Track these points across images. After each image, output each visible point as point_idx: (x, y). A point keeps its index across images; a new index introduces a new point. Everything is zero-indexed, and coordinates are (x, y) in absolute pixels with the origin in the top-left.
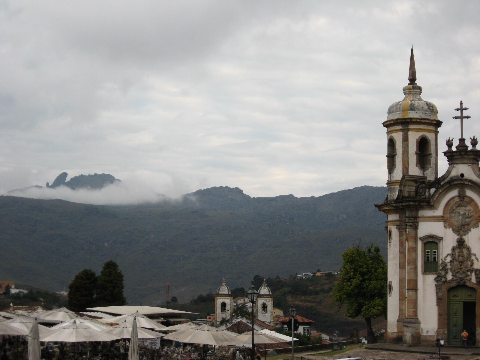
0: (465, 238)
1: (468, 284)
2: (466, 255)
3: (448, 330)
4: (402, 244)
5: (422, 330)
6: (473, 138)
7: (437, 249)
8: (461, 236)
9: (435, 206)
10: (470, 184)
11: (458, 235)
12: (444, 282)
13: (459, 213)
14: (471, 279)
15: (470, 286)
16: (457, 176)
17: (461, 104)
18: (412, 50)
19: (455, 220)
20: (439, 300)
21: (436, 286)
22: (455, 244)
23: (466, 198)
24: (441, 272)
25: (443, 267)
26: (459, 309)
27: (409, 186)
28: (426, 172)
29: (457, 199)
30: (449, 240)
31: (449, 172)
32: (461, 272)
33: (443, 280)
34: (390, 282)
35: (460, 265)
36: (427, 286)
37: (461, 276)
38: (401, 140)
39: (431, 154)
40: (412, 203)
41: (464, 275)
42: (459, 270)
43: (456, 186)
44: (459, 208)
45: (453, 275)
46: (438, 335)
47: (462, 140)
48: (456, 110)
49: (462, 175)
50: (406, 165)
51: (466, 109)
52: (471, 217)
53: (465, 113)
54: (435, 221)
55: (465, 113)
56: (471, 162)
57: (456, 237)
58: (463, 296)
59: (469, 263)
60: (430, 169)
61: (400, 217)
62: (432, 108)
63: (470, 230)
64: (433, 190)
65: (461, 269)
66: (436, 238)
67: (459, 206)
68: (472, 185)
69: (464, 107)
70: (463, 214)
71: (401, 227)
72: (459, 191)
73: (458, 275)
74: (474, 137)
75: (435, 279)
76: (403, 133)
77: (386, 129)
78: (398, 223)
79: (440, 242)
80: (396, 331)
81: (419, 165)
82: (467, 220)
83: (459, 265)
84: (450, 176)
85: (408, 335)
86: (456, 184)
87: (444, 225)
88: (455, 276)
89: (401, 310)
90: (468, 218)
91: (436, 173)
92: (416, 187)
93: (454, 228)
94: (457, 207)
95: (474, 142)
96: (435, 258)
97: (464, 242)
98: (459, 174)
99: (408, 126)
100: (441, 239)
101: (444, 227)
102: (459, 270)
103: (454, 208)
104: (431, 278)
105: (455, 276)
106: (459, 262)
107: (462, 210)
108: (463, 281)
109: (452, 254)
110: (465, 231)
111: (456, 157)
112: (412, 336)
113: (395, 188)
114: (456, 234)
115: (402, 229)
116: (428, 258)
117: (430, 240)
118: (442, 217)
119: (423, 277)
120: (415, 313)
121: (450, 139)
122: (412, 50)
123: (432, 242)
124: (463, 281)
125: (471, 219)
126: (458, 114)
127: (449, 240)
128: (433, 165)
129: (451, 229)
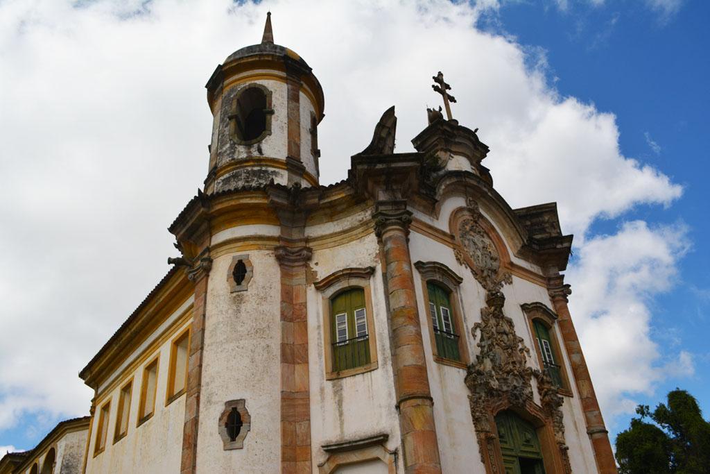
10: (489, 194)
11: (484, 287)
14: (532, 393)
15: (533, 414)
17: (440, 74)
18: (269, 14)
19: (471, 254)
20: (486, 443)
29: (466, 215)
37: (515, 383)
50: (296, 139)
52: (495, 260)
53: (448, 91)
54: (436, 238)
61: (282, 232)
72: (470, 200)
76: (290, 86)
84: (446, 169)
86: (466, 185)
87: (456, 257)
90: (492, 258)
94: (471, 230)
101: (458, 259)
106: (506, 348)
109: (483, 325)
113: (266, 171)
114: (481, 283)
115: (289, 260)
122: (269, 14)
123: (441, 285)
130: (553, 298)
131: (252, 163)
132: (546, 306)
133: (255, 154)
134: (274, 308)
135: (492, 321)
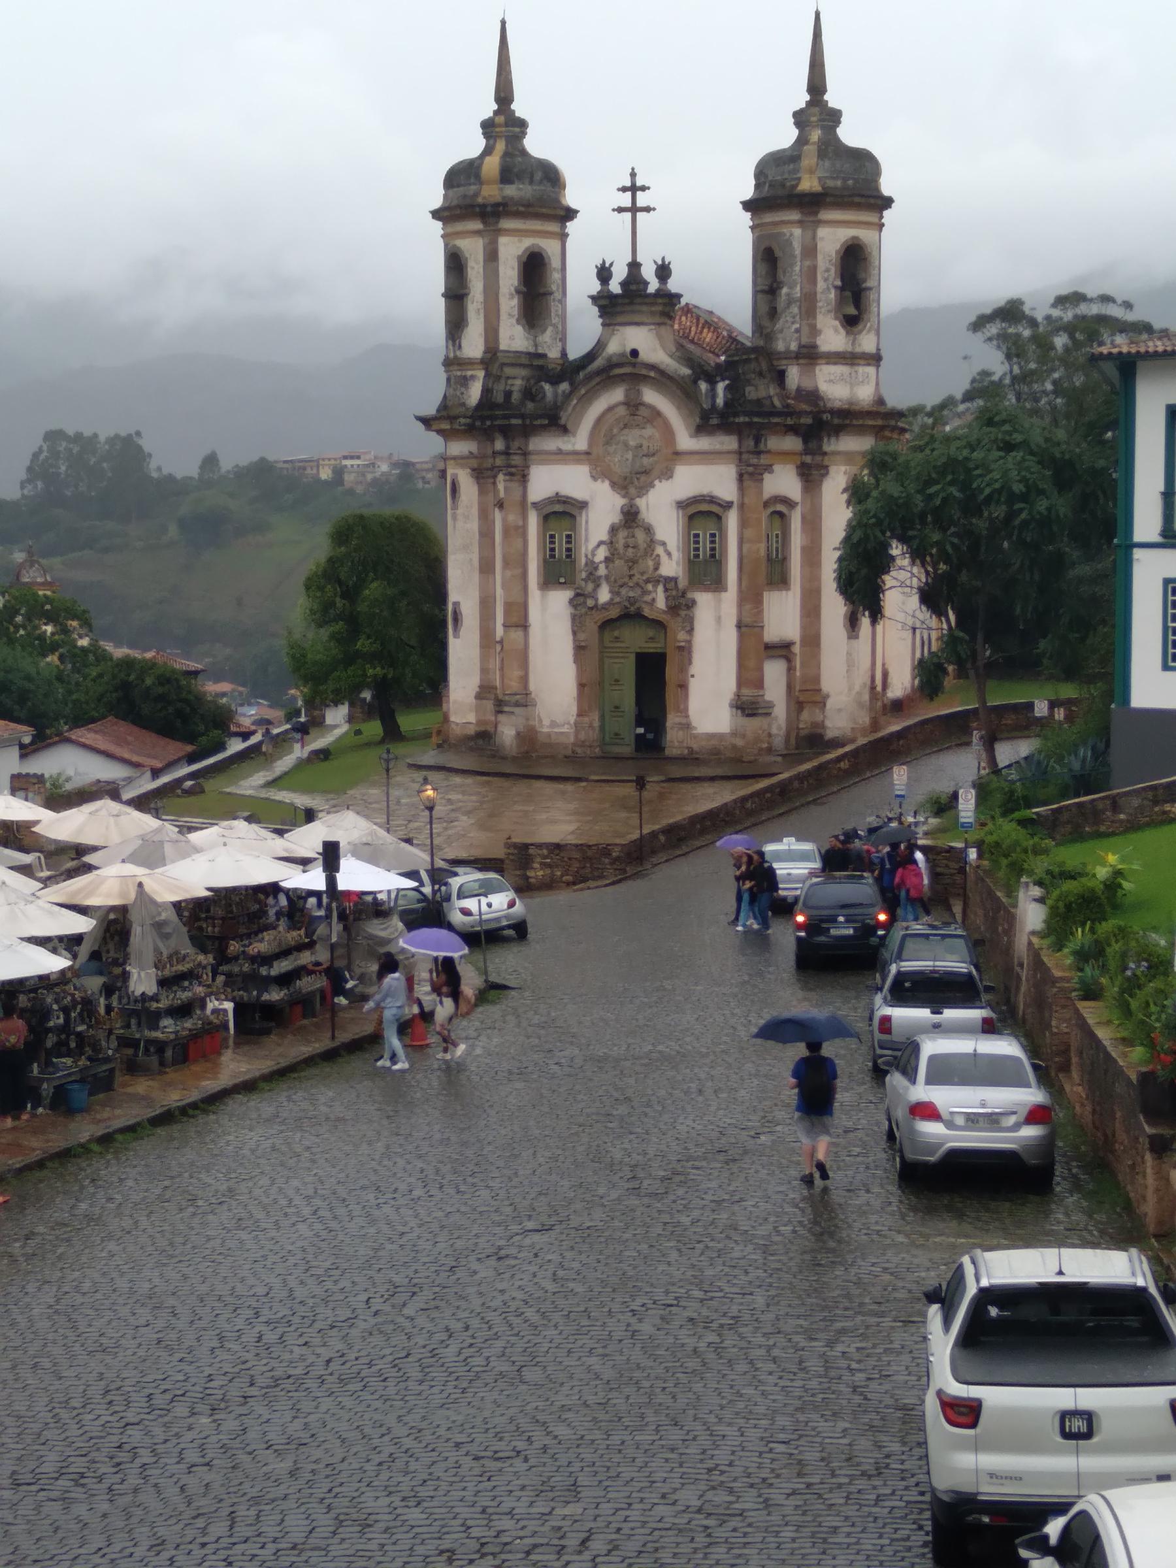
0: (641, 503)
1: (647, 612)
2: (642, 546)
3: (602, 718)
4: (485, 516)
5: (541, 721)
6: (660, 262)
7: (573, 527)
8: (632, 499)
9: (569, 427)
10: (652, 374)
11: (624, 497)
12: (591, 608)
13: (626, 445)
14: (654, 600)
16: (623, 355)
17: (633, 175)
18: (503, 23)
20: (580, 649)
21: (574, 618)
22: (615, 517)
23: (642, 408)
24: (583, 583)
25: (591, 574)
26: (627, 669)
27: (508, 378)
28: (540, 339)
29: (622, 411)
30: (602, 510)
31: (600, 345)
32: (631, 584)
33: (590, 603)
34: (456, 604)
35: (630, 568)
36: (551, 618)
37: (631, 594)
38: (481, 258)
39: (551, 294)
40: (514, 421)
41: (639, 591)
42: (626, 580)
43: (622, 378)
44: (626, 431)
45: (611, 592)
46: (577, 733)
47: (634, 266)
48: (619, 190)
49: (635, 353)
51: (644, 188)
52: (654, 455)
55: (642, 199)
56: (657, 319)
57: (619, 501)
58: (636, 639)
59: (651, 563)
60: (550, 329)
62: (551, 176)
63: (652, 485)
64: (564, 386)
65: (631, 576)
66: (573, 505)
67: (625, 426)
68: (658, 376)
69: (639, 184)
70: (636, 447)
71: (483, 475)
73: (624, 591)
74: (663, 259)
75: (571, 601)
77: (439, 224)
78: (474, 463)
79: (581, 514)
80: (472, 718)
81: (524, 321)
82: (645, 461)
83: (626, 568)
85: (507, 733)
88: (618, 593)
89: (484, 671)
91: (563, 340)
92: (523, 379)
93: (615, 480)
95: (663, 271)
96: (569, 550)
97: (637, 513)
98: (628, 350)
99: (497, 222)
100: (583, 505)
101: (592, 477)
102: (626, 580)
103: (615, 431)
104: (560, 599)
105: (618, 593)
107: (633, 437)
108: (637, 605)
110: (641, 488)
111: (619, 309)
112: (518, 734)
116: (552, 550)
117: (558, 508)
118: (587, 453)
119: (543, 596)
120: (525, 680)
121: (604, 262)
122: (503, 23)
123: (563, 513)
124: (637, 605)
125: (655, 458)
126: (625, 200)
127: (602, 510)
128: (555, 320)
129: (607, 483)
130: (741, 478)
131: (456, 367)
132: (712, 497)
133: (458, 353)
134: (474, 525)
135: (622, 534)
